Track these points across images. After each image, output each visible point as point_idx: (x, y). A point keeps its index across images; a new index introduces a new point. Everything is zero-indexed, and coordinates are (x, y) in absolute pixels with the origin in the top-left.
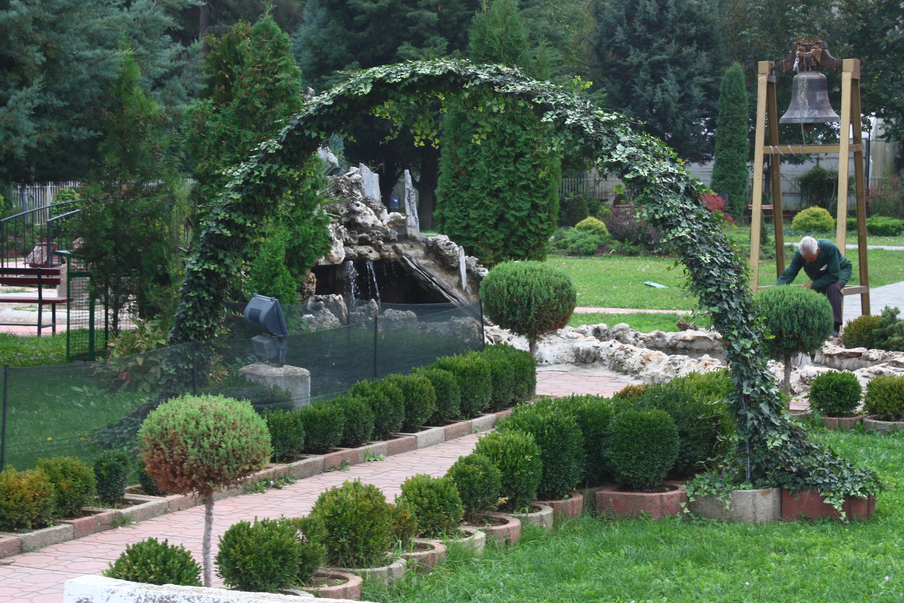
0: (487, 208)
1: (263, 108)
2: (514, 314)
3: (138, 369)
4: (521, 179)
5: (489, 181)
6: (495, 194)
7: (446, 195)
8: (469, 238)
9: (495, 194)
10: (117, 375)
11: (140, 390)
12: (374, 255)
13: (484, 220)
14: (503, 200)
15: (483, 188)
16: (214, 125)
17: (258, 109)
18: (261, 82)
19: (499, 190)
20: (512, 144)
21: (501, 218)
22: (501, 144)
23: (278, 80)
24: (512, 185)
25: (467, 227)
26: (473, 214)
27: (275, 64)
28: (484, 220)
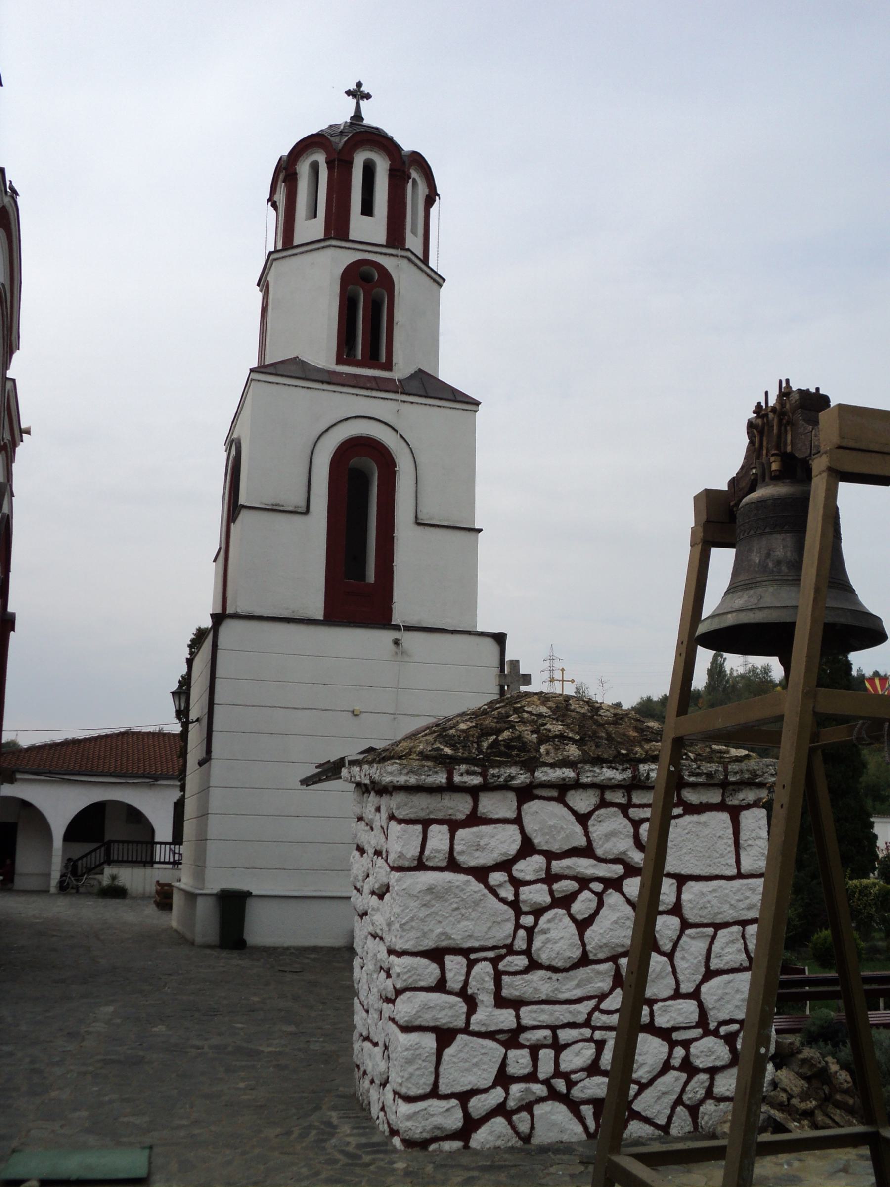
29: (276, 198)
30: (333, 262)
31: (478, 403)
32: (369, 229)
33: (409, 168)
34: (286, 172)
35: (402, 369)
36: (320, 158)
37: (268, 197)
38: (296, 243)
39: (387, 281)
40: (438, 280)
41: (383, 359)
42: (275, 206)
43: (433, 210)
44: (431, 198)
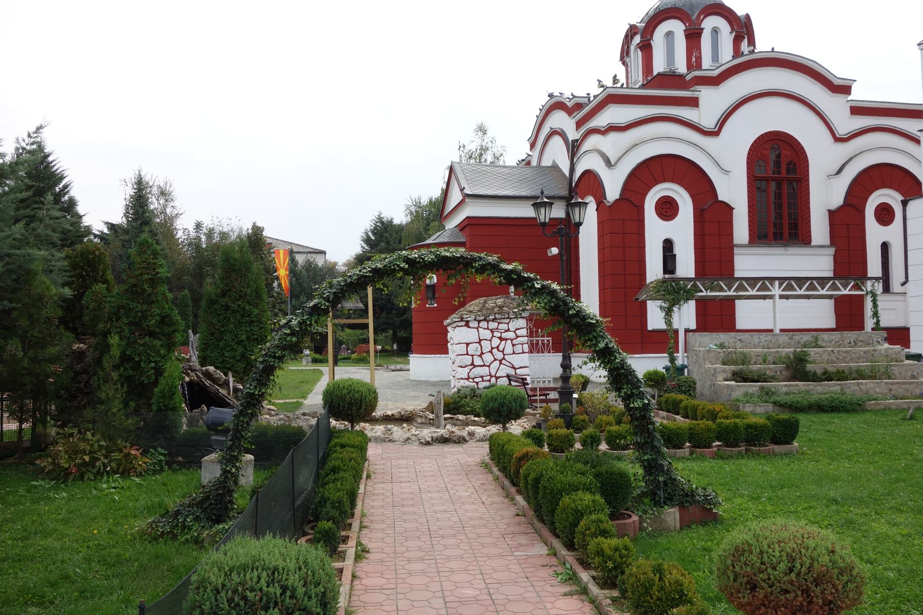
0: (236, 351)
1: (149, 290)
2: (351, 410)
3: (85, 464)
4: (254, 334)
5: (236, 336)
6: (240, 343)
7: (206, 344)
8: (224, 368)
9: (240, 343)
10: (67, 469)
11: (86, 478)
12: (187, 379)
13: (234, 357)
14: (244, 346)
15: (233, 340)
16: (113, 300)
17: (144, 290)
18: (148, 274)
19: (242, 341)
20: (249, 316)
21: (243, 356)
22: (243, 316)
23: (158, 273)
24: (248, 338)
25: (223, 361)
26: (227, 354)
27: (155, 264)
28: (234, 357)
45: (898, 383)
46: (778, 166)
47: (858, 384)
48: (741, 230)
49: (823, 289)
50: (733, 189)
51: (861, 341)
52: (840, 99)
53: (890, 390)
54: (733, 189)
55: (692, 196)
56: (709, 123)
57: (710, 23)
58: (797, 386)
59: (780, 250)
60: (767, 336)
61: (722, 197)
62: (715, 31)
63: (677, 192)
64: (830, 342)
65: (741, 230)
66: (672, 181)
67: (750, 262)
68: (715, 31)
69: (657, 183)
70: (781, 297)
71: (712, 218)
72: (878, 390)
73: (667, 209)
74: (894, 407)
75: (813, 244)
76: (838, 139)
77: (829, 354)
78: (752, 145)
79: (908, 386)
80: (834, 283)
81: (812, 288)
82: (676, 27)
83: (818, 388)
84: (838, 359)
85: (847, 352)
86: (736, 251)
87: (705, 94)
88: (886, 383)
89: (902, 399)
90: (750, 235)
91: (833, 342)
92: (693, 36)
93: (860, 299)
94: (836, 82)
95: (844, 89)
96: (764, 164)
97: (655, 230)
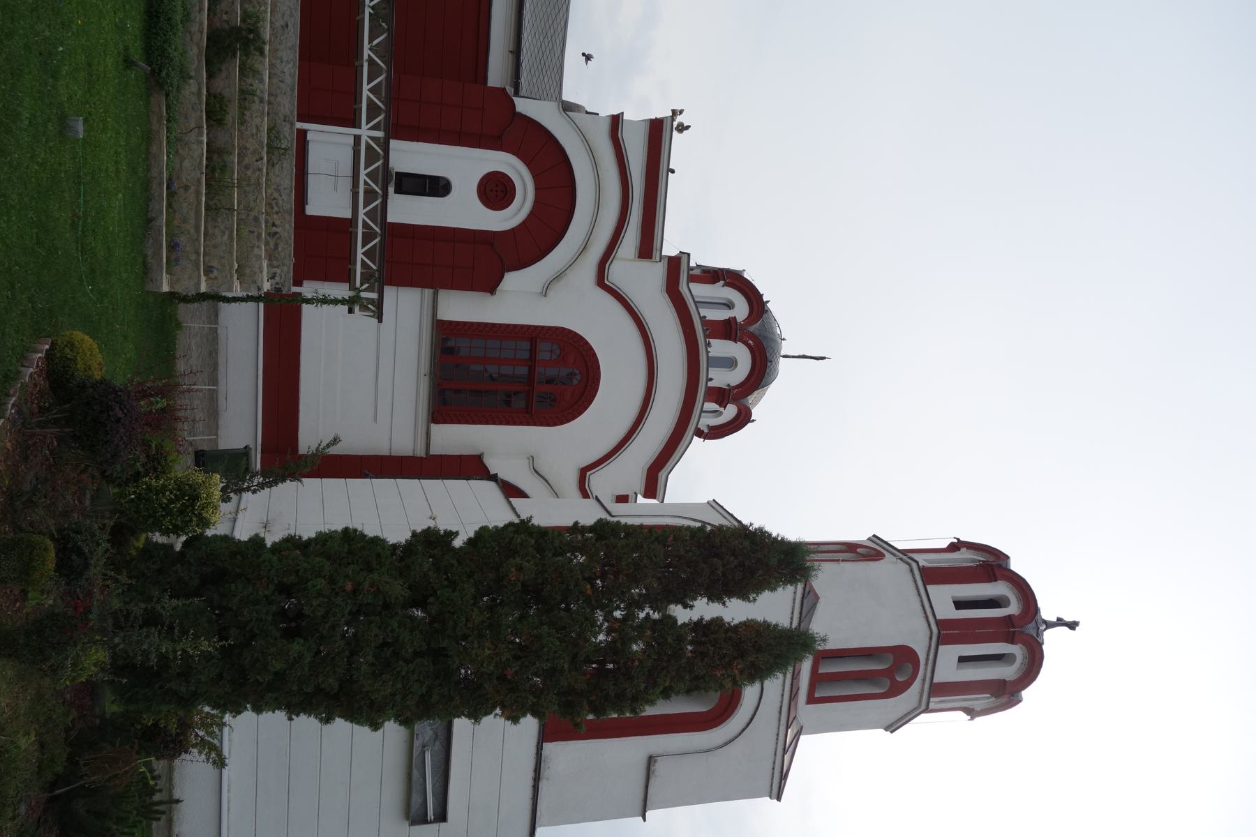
29: (963, 550)
30: (916, 636)
31: (779, 799)
32: (948, 665)
33: (1005, 694)
34: (992, 564)
35: (805, 711)
36: (1013, 609)
37: (962, 539)
38: (929, 587)
39: (896, 690)
40: (892, 727)
41: (817, 695)
42: (956, 546)
43: (961, 715)
44: (972, 713)
45: (199, 202)
46: (550, 378)
47: (200, 127)
48: (461, 307)
49: (370, 90)
50: (520, 300)
51: (276, 245)
52: (636, 480)
53: (186, 188)
54: (520, 300)
55: (513, 229)
56: (618, 273)
57: (740, 353)
58: (201, 10)
59: (425, 367)
60: (292, 76)
61: (512, 280)
62: (731, 363)
63: (519, 210)
64: (277, 190)
65: (461, 307)
66: (537, 202)
67: (406, 307)
68: (731, 363)
69: (535, 176)
70: (357, 139)
71: (482, 260)
72: (187, 163)
73: (495, 191)
74: (154, 149)
75: (433, 426)
76: (584, 473)
77: (254, 152)
78: (582, 338)
79: (192, 222)
80: (374, 236)
81: (370, 194)
82: (741, 311)
83: (195, 50)
84: (247, 167)
85: (258, 184)
86: (428, 292)
87: (655, 273)
88: (199, 181)
89: (169, 205)
90: (451, 323)
91: (276, 195)
92: (727, 330)
93: (347, 277)
94: (662, 474)
95: (652, 487)
96: (554, 357)
97: (466, 165)
